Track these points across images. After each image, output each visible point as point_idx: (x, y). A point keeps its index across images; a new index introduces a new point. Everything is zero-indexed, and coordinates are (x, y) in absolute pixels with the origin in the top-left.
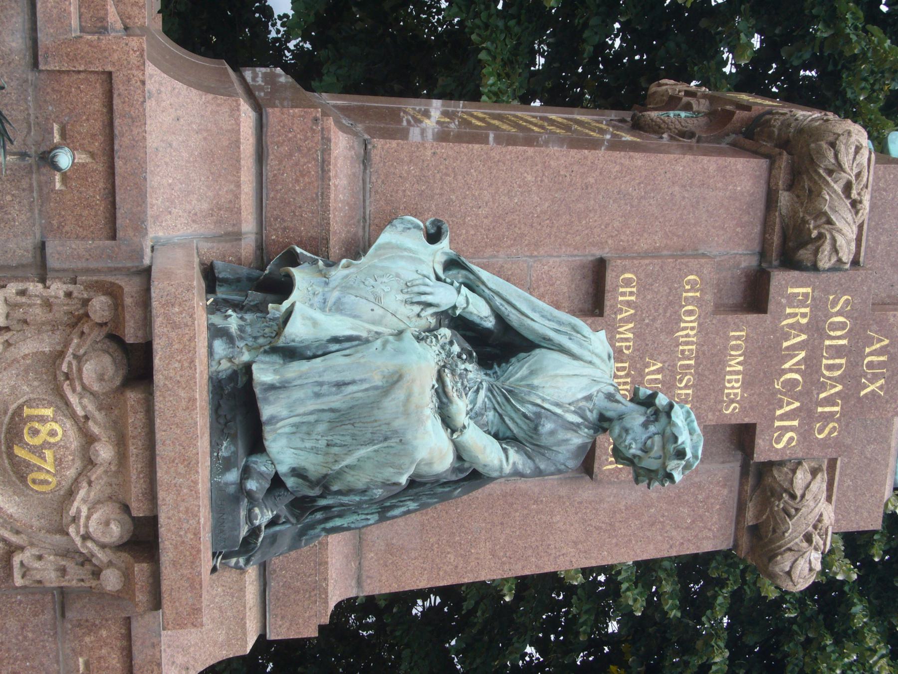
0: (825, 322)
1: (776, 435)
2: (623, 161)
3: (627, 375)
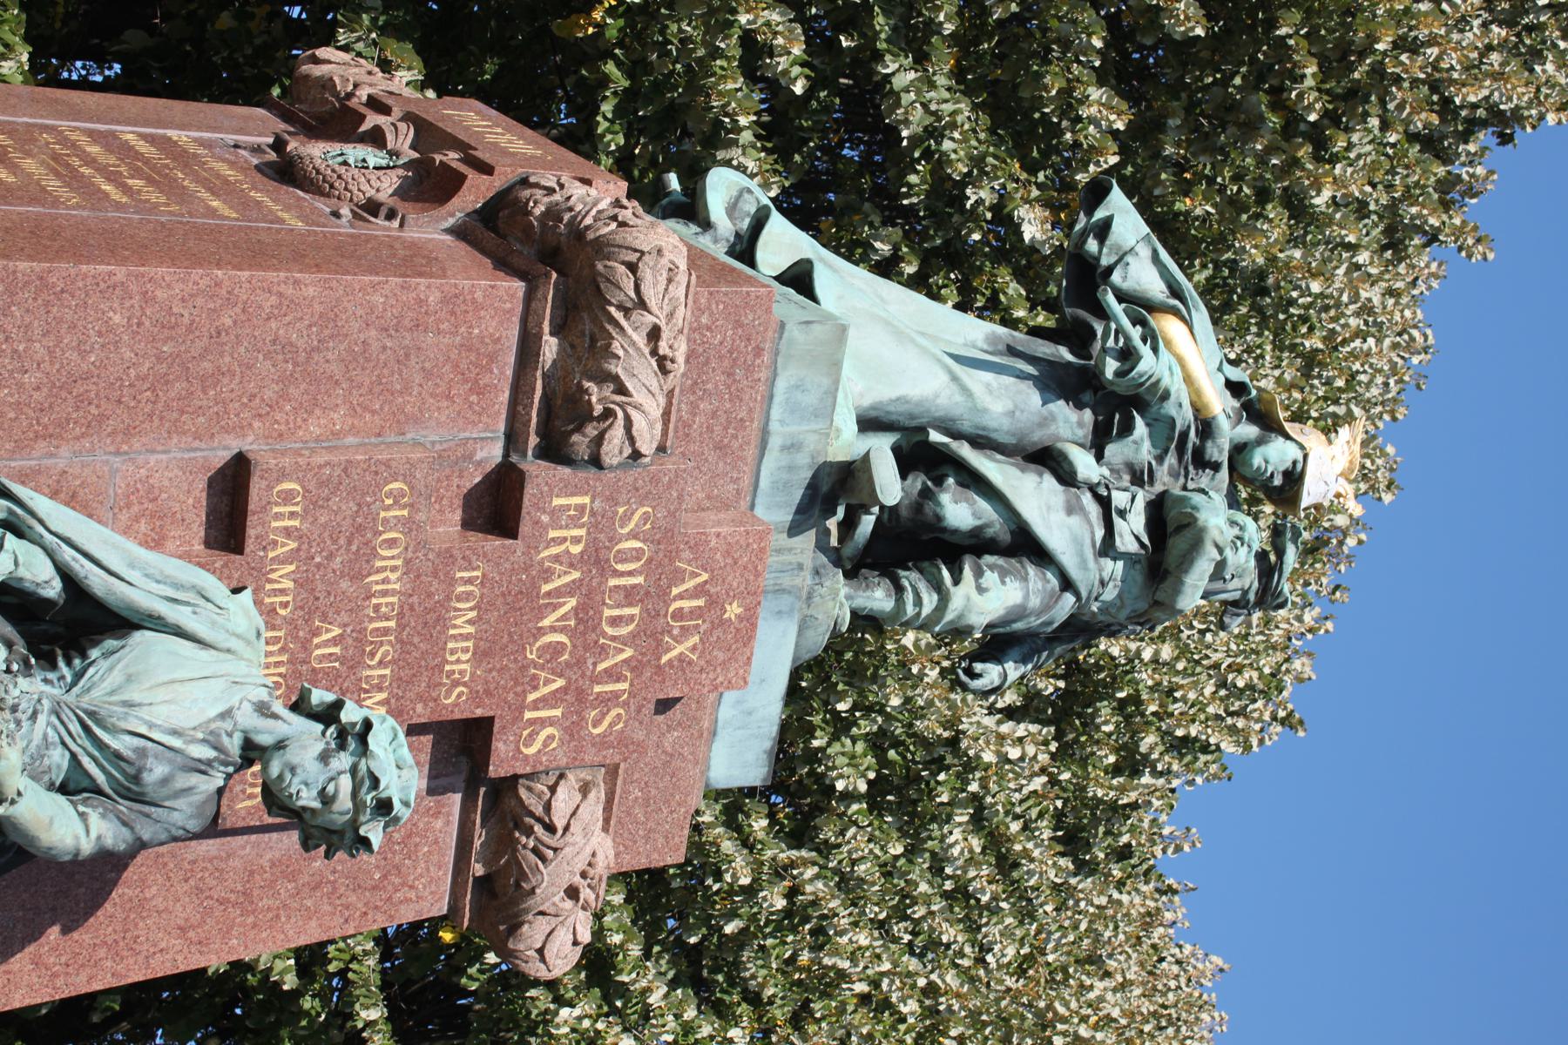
0: (609, 549)
1: (525, 733)
2: (282, 288)
3: (282, 650)
